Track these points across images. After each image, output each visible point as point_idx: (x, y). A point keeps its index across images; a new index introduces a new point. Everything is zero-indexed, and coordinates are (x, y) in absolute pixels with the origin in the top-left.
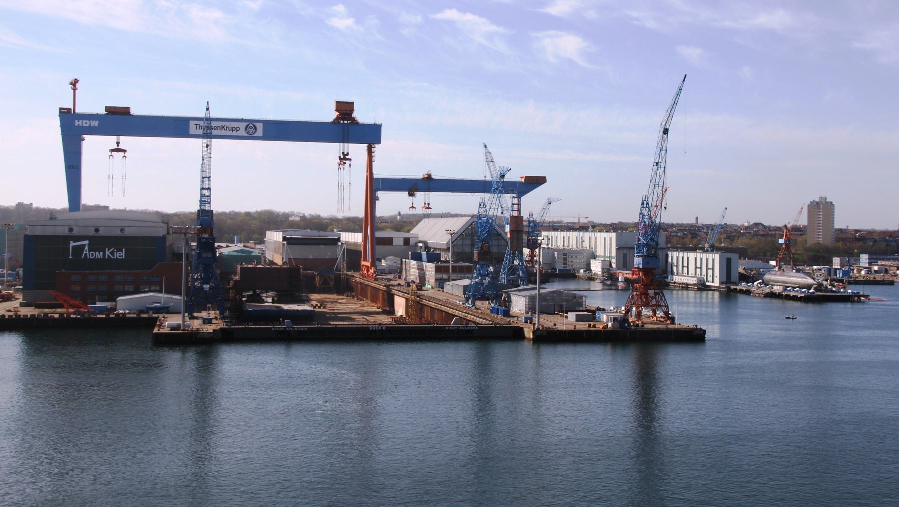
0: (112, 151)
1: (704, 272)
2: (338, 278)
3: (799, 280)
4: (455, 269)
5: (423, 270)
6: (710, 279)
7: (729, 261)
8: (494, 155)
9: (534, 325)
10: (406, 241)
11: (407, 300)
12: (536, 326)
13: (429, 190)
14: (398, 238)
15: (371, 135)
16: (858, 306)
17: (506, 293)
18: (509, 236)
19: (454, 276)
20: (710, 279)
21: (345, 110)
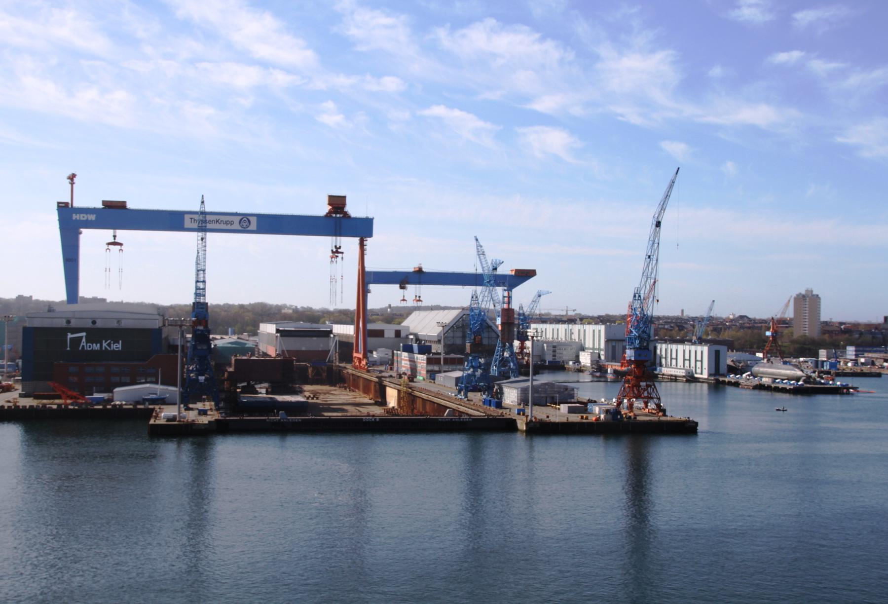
0: (109, 244)
1: (693, 364)
2: (330, 370)
3: (788, 372)
4: (447, 361)
5: (414, 362)
6: (699, 371)
7: (717, 353)
8: (485, 248)
9: (527, 416)
10: (398, 333)
11: (399, 391)
12: (529, 418)
13: (420, 282)
14: (389, 331)
15: (362, 229)
16: (846, 398)
17: (498, 385)
18: (500, 328)
19: (446, 368)
20: (699, 371)
21: (337, 204)
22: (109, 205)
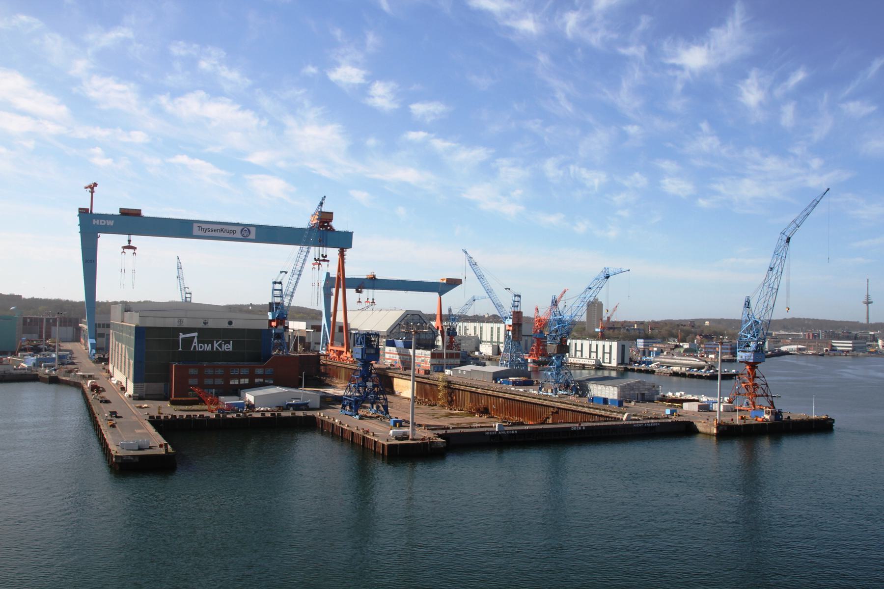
0: (124, 247)
6: (607, 360)
7: (623, 346)
13: (373, 288)
15: (344, 241)
20: (607, 360)
21: (325, 219)
22: (125, 212)
